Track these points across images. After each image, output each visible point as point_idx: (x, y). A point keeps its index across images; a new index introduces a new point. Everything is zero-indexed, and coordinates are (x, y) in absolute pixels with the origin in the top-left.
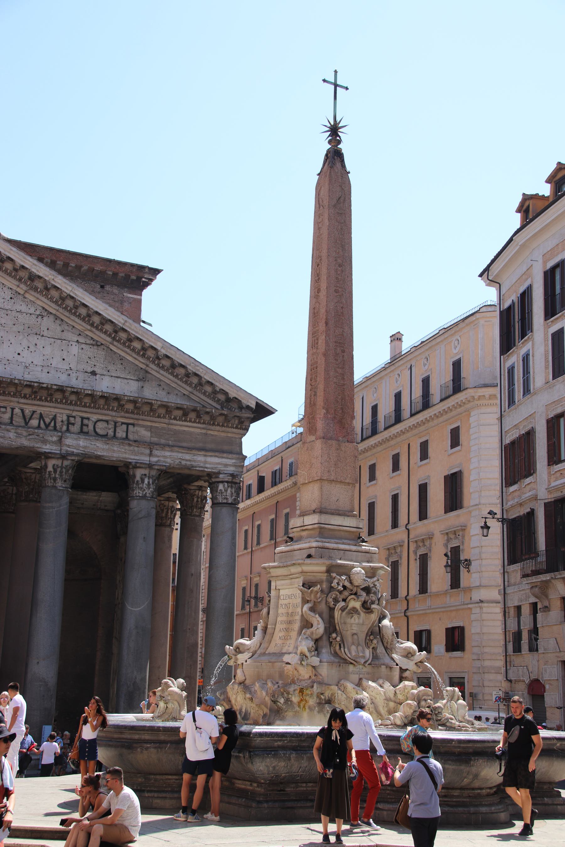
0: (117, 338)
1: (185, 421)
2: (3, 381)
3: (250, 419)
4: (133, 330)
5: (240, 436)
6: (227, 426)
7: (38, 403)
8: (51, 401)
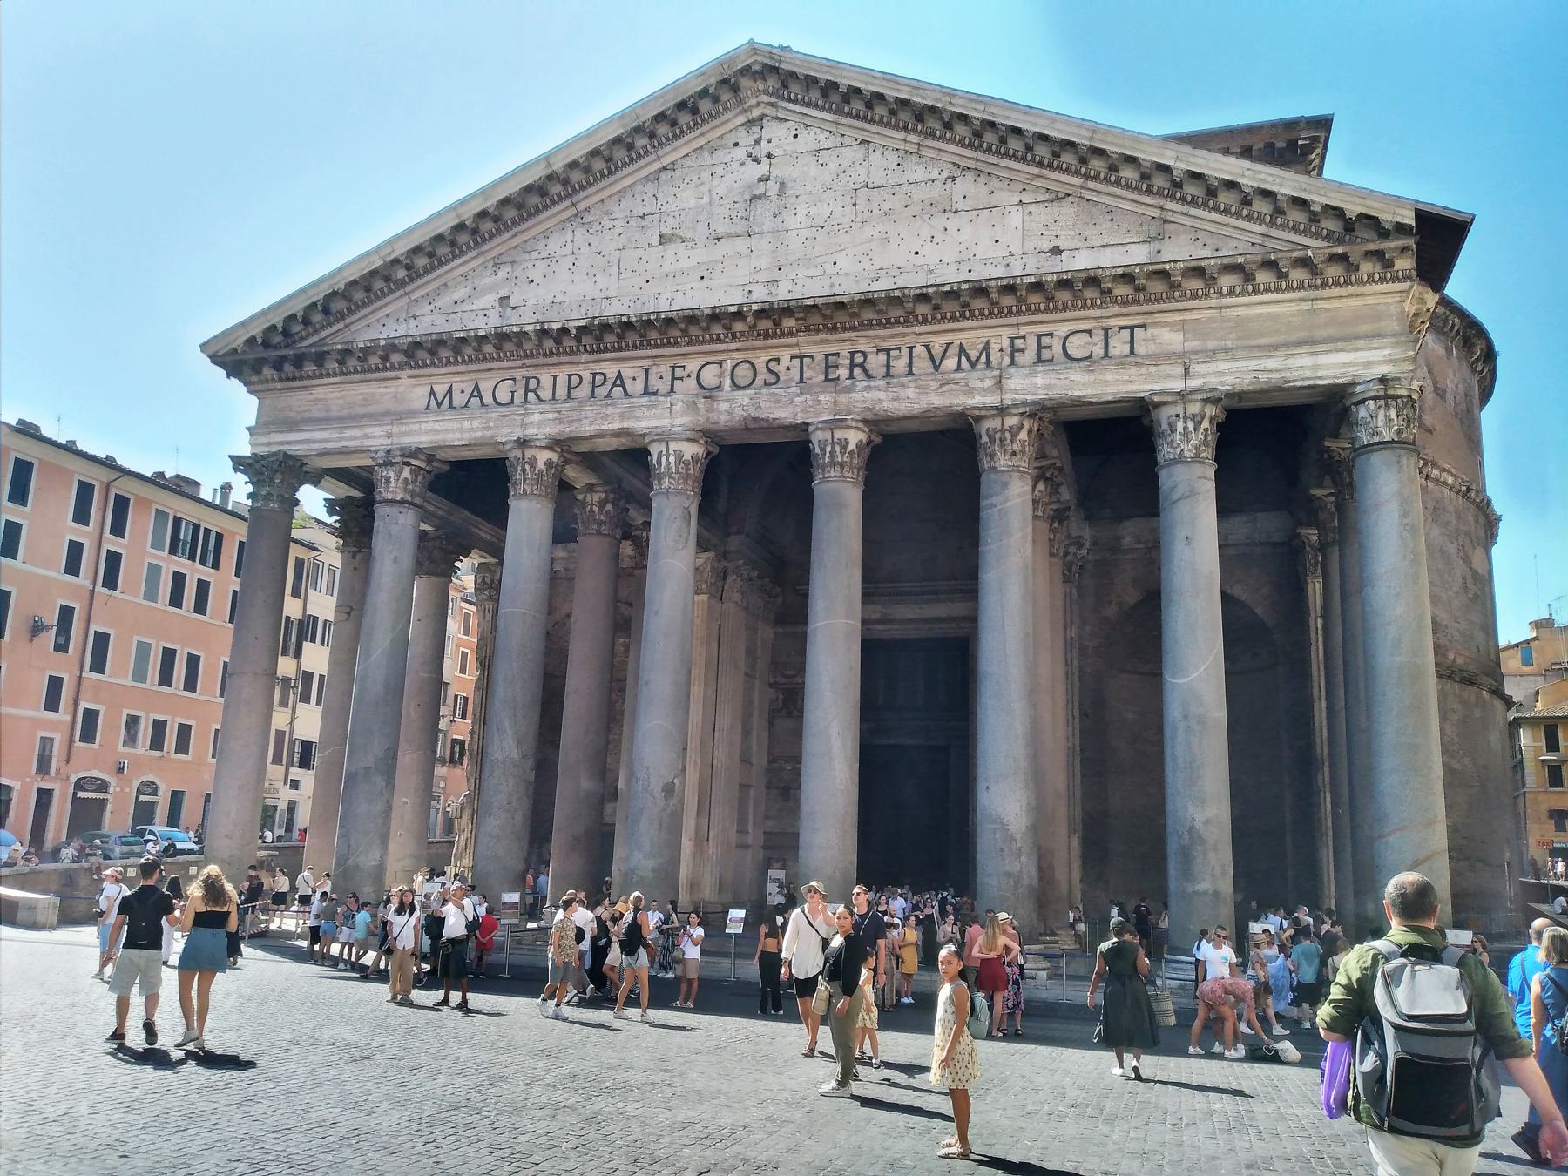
1: (1256, 292)
2: (877, 299)
4: (1112, 144)
5: (1397, 298)
6: (1360, 282)
8: (972, 316)
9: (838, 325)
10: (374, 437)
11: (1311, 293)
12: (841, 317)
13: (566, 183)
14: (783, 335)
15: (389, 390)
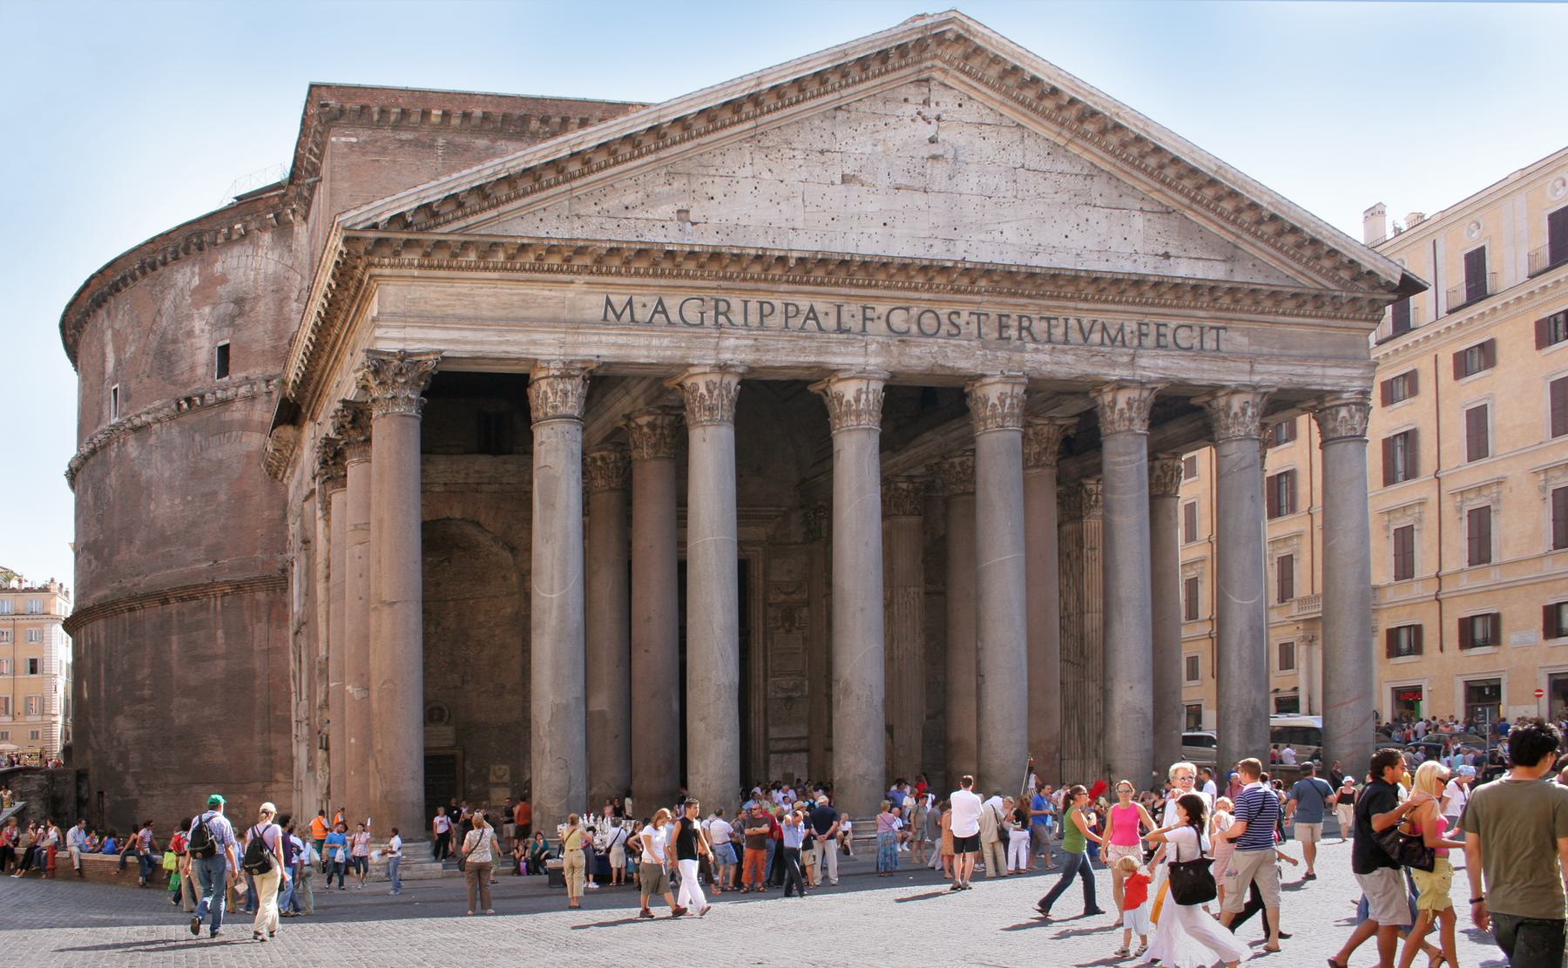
1: (1298, 315)
6: (1354, 319)
10: (542, 344)
11: (1326, 322)
12: (1028, 288)
14: (971, 292)
15: (553, 293)
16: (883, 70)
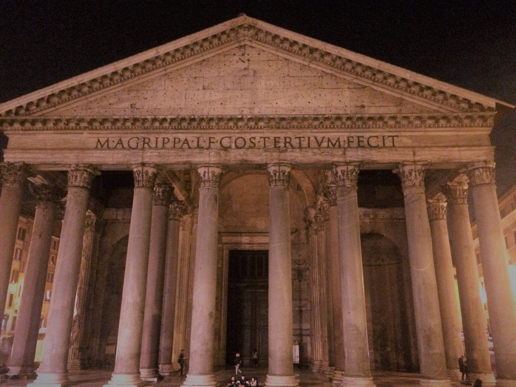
0: (377, 80)
1: (438, 127)
3: (492, 118)
7: (327, 130)
8: (334, 128)
9: (281, 126)
11: (458, 129)
13: (164, 60)
14: (258, 128)
15: (76, 138)
16: (220, 44)
